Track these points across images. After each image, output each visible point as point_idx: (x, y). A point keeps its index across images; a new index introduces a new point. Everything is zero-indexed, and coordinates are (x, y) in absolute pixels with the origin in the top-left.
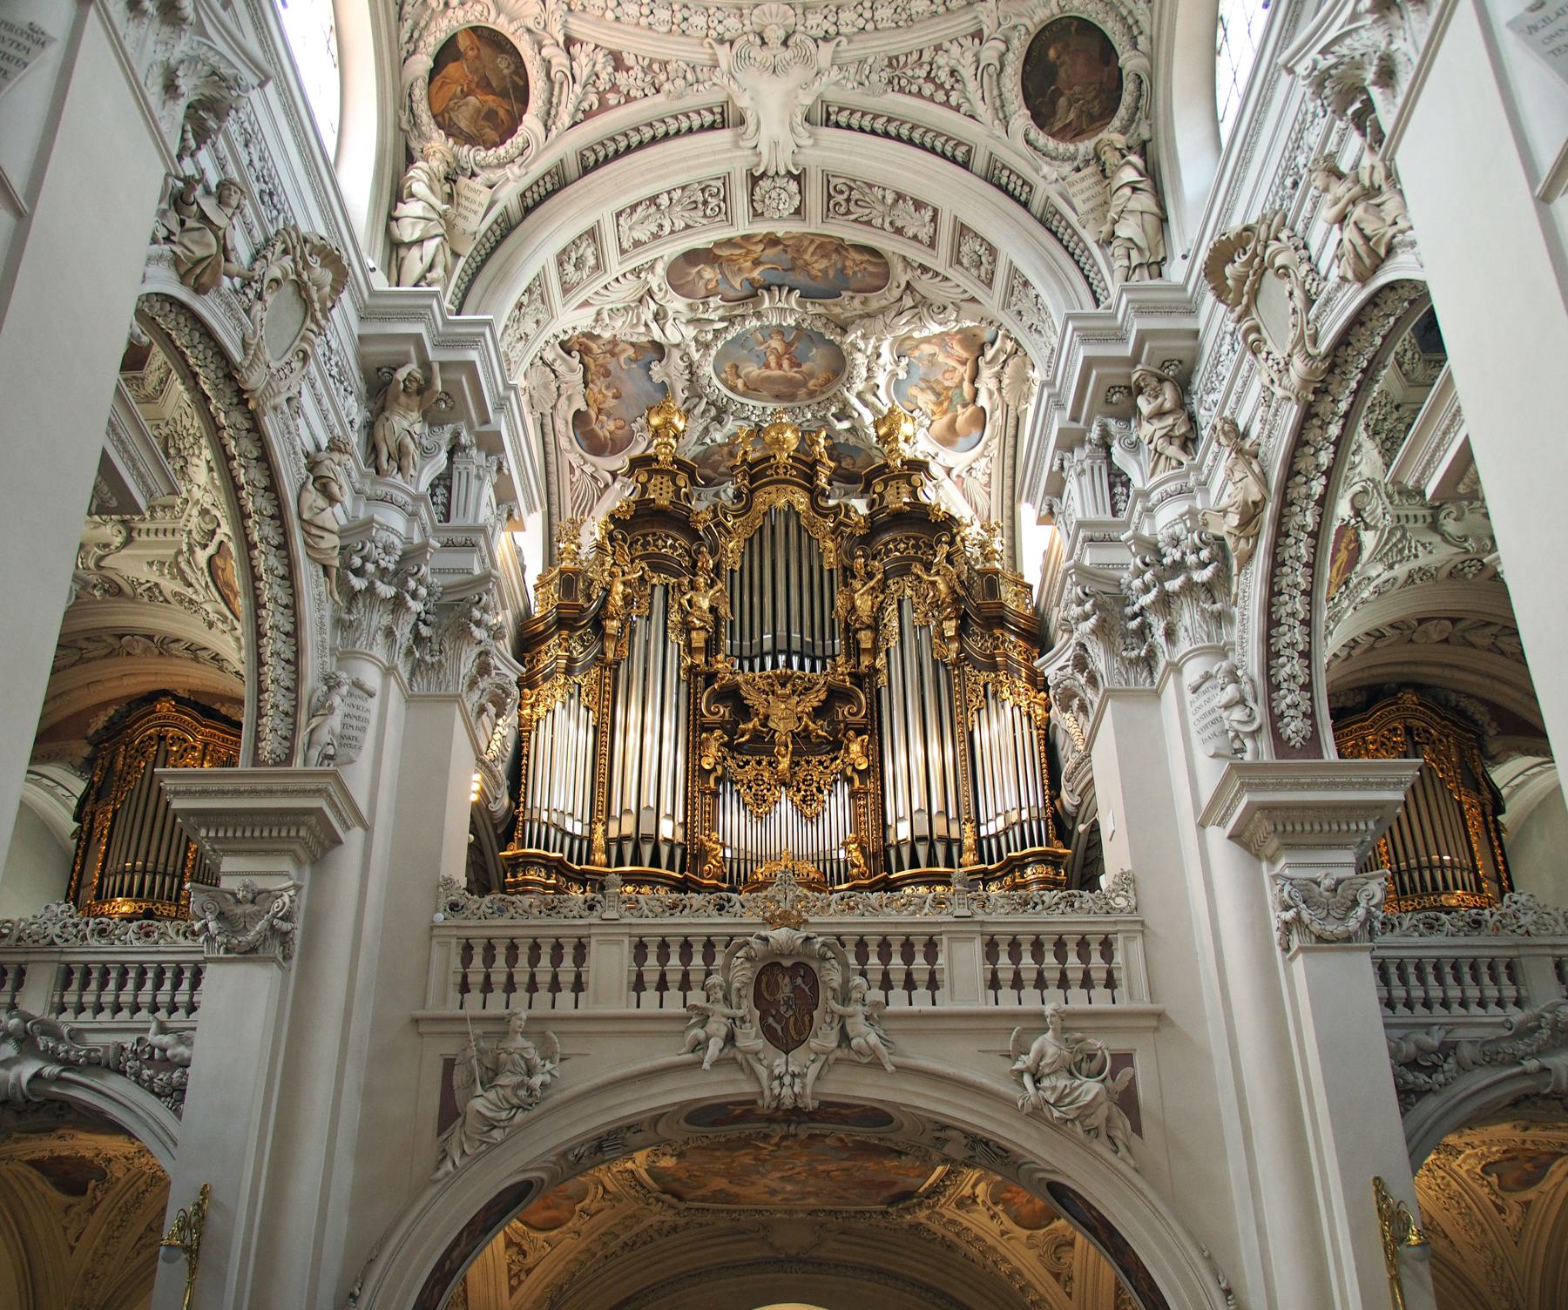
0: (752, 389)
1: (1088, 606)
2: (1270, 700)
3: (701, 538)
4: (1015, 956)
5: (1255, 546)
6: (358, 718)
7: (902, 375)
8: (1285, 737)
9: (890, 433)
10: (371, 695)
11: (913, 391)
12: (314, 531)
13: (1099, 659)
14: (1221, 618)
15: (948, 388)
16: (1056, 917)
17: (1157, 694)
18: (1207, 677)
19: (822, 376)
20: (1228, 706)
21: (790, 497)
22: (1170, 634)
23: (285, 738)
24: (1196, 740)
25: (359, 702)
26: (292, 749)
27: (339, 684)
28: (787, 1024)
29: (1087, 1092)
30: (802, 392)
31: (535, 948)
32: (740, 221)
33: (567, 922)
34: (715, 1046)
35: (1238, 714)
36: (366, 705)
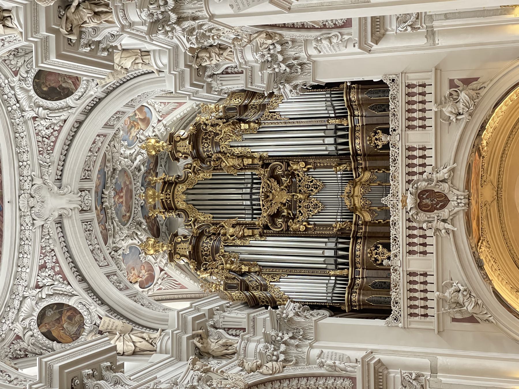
0: (129, 210)
1: (281, 87)
2: (329, 28)
3: (203, 231)
4: (413, 119)
5: (277, 34)
6: (332, 356)
7: (126, 143)
8: (343, 24)
9: (154, 149)
10: (322, 352)
11: (131, 138)
12: (274, 370)
13: (299, 82)
14: (293, 41)
15: (130, 122)
16: (400, 104)
17: (314, 62)
18: (316, 48)
19: (126, 178)
20: (331, 43)
21: (180, 193)
22: (295, 59)
23: (344, 380)
24: (338, 52)
25: (326, 355)
26: (347, 377)
27: (322, 362)
28: (439, 201)
29: (465, 97)
30: (130, 187)
31: (410, 290)
32: (90, 216)
33: (402, 279)
34: (447, 226)
35: (334, 40)
36: (326, 353)
